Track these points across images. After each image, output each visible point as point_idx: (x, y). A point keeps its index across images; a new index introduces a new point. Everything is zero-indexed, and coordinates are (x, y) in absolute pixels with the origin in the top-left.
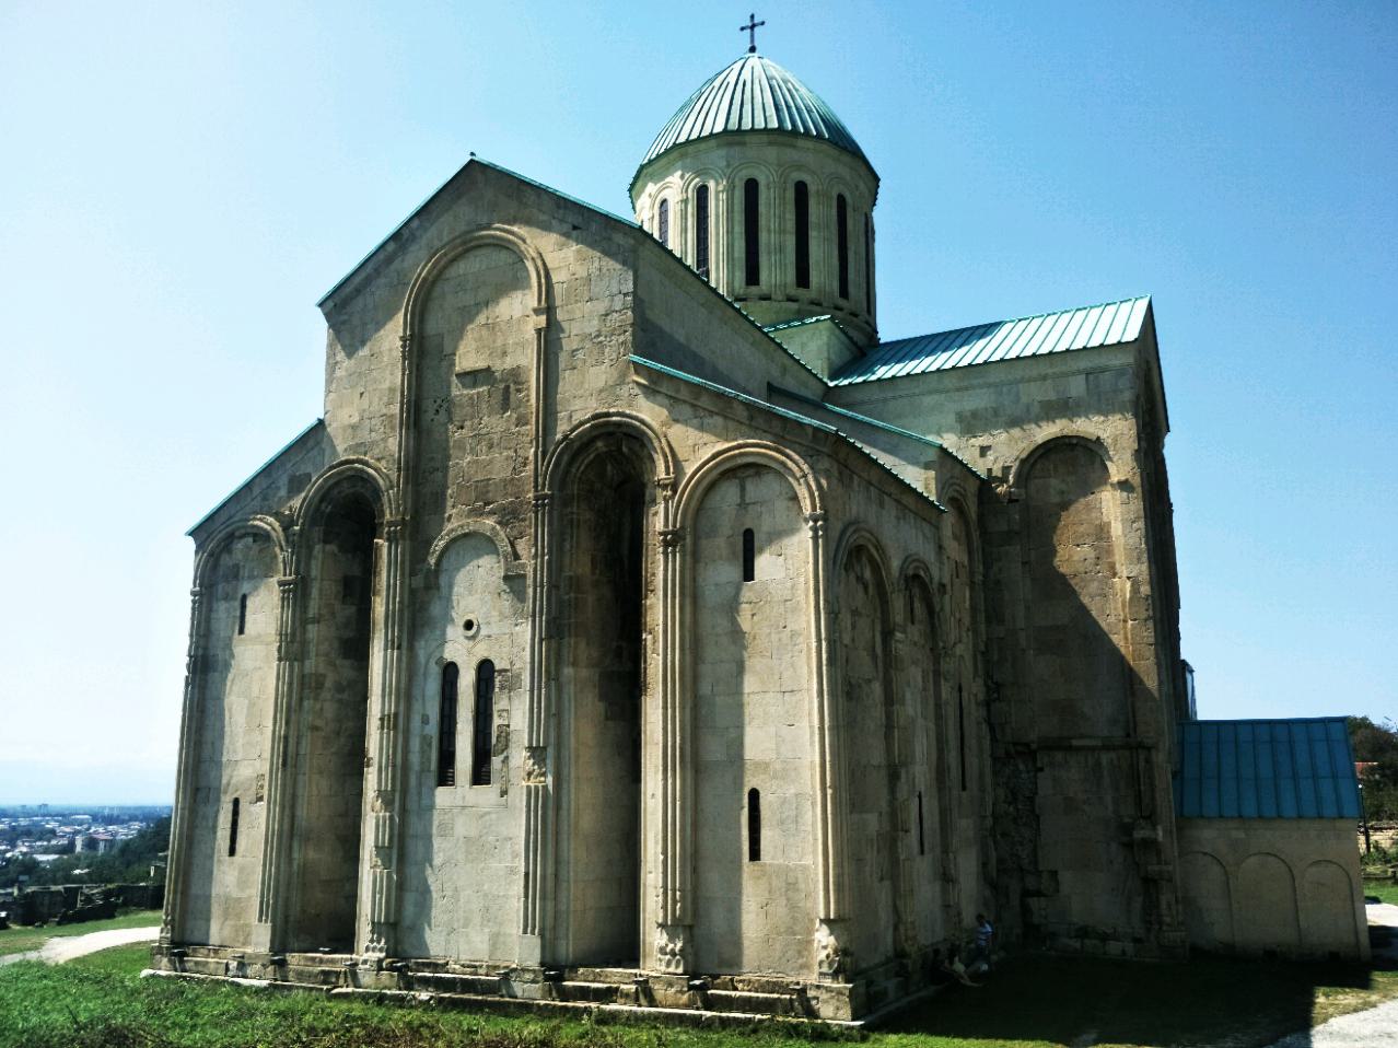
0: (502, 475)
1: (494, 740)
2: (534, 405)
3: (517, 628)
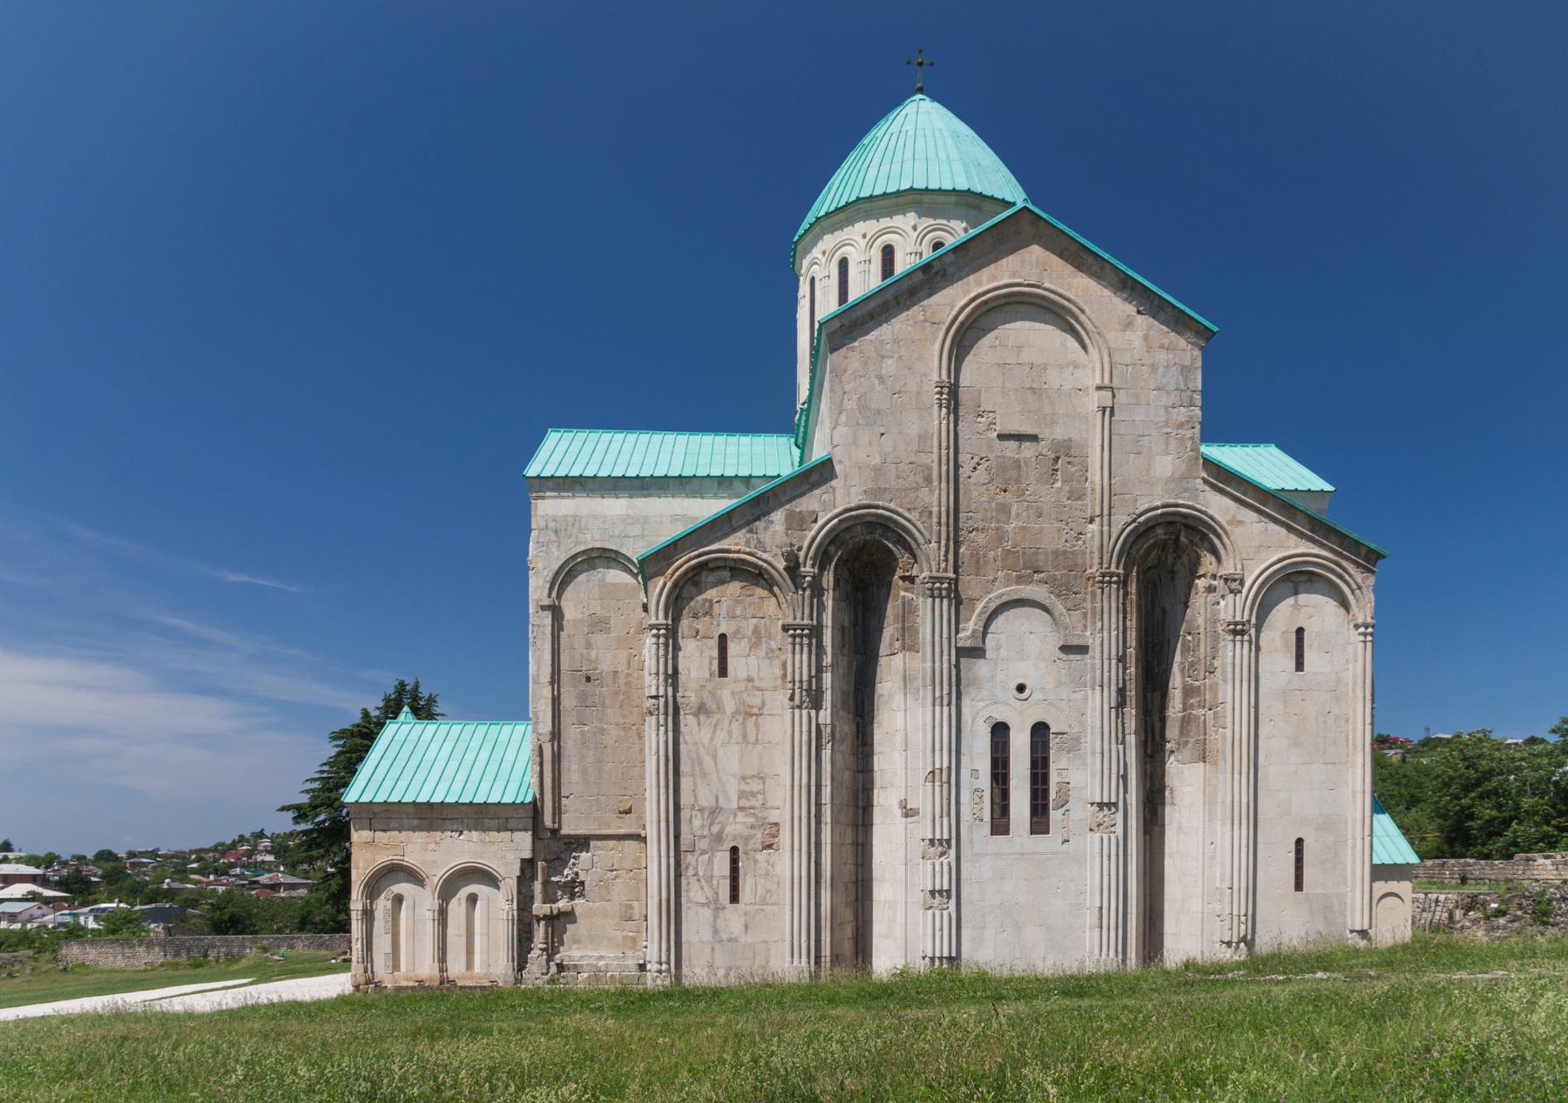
0: (1053, 547)
1: (1052, 795)
3: (1075, 695)
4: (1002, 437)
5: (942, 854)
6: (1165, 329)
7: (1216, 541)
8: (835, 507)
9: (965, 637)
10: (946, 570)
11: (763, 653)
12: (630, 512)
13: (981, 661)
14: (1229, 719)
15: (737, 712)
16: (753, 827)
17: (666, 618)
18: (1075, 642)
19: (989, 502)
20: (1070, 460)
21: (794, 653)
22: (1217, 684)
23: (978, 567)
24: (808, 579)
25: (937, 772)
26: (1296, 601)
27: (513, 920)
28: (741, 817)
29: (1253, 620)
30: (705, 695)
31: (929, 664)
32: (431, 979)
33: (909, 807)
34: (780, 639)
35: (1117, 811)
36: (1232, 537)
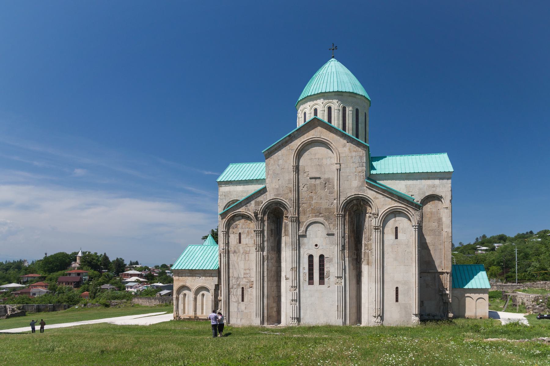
0: (325, 207)
1: (325, 274)
2: (336, 189)
3: (331, 247)
4: (311, 178)
5: (295, 290)
6: (355, 146)
7: (370, 203)
8: (267, 199)
9: (301, 232)
10: (295, 215)
11: (249, 237)
12: (243, 189)
13: (306, 238)
14: (374, 254)
15: (243, 253)
16: (247, 282)
17: (226, 229)
18: (330, 233)
19: (307, 196)
20: (329, 183)
21: (256, 237)
22: (371, 243)
23: (305, 213)
24: (260, 218)
25: (293, 268)
26: (395, 219)
27: (213, 301)
28: (244, 280)
29: (381, 225)
30: (236, 248)
31: (291, 240)
32: (192, 316)
33: (287, 277)
34: (254, 234)
35: (342, 279)
36: (375, 202)
